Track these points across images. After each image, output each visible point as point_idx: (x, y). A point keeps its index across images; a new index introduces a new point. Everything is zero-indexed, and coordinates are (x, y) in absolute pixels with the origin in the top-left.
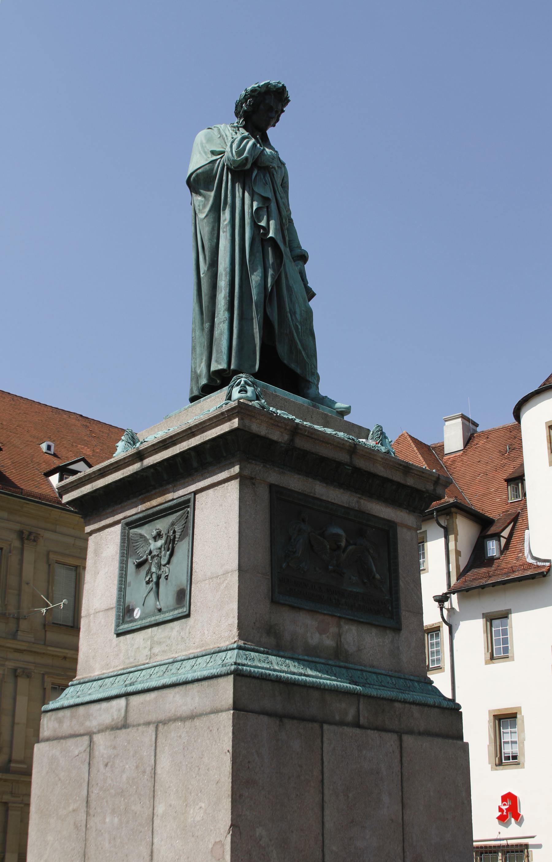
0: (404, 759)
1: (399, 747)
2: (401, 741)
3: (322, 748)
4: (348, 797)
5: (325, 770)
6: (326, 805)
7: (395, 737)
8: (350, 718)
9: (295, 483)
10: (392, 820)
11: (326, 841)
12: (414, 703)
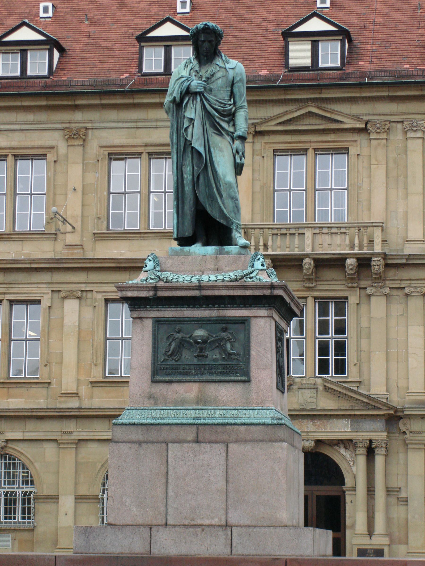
0: (229, 457)
1: (226, 451)
2: (227, 447)
3: (167, 456)
4: (185, 480)
5: (169, 466)
6: (169, 485)
7: (221, 446)
8: (190, 438)
9: (169, 313)
10: (218, 490)
11: (169, 503)
12: (243, 424)
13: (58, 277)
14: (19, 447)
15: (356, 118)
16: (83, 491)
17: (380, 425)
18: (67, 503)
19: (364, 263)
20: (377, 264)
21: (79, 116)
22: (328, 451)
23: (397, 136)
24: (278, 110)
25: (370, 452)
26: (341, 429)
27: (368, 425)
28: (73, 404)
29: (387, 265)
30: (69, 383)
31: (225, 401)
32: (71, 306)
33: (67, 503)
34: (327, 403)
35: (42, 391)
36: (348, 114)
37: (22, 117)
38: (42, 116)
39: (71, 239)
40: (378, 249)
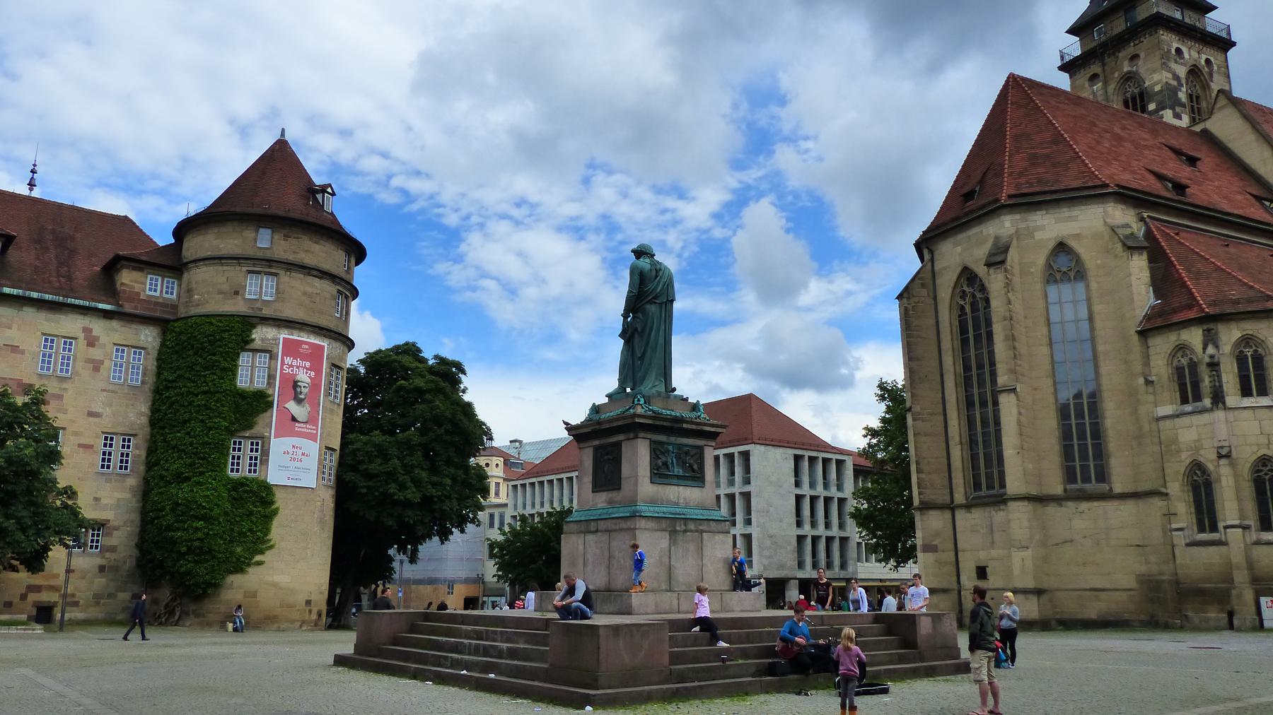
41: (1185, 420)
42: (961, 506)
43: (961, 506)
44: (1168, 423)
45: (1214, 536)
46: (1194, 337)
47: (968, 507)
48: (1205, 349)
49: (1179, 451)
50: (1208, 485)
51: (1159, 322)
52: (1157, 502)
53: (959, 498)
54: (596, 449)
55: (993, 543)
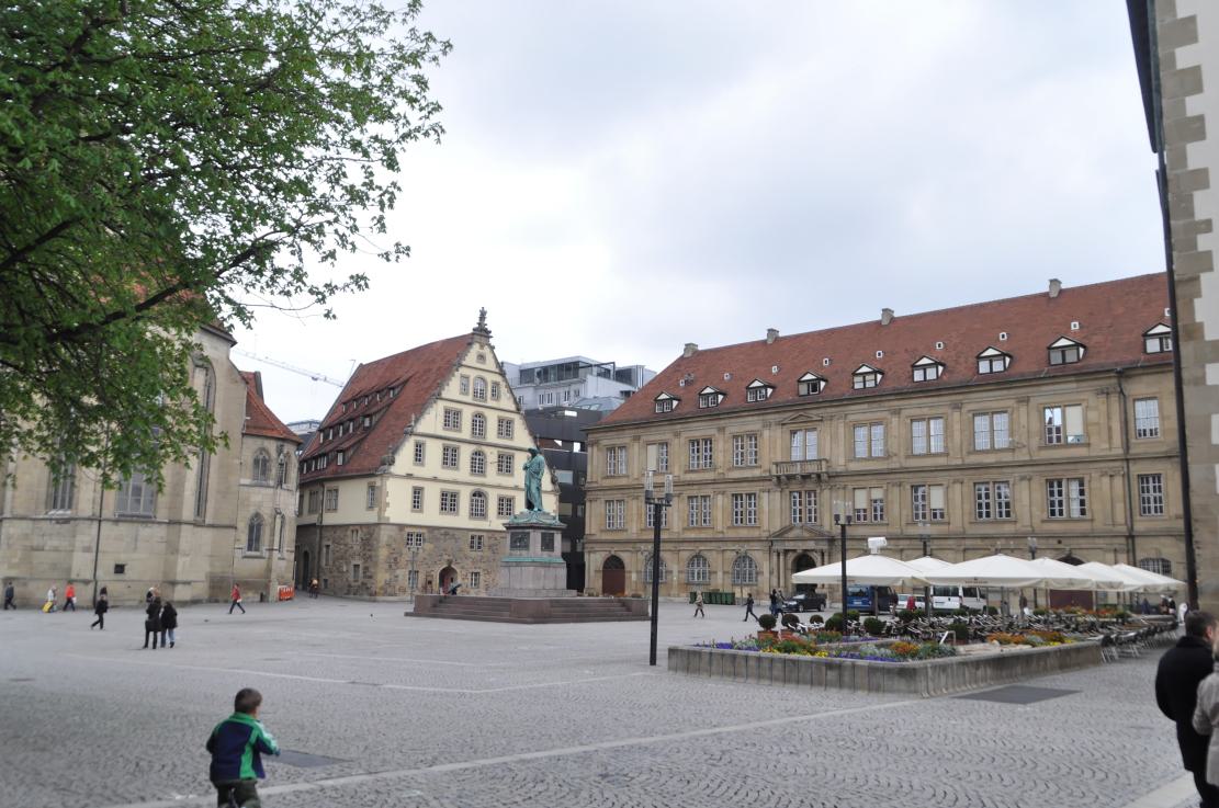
9: (513, 531)
13: (716, 486)
14: (753, 553)
15: (817, 415)
16: (726, 569)
17: (825, 543)
18: (720, 574)
19: (819, 476)
20: (824, 477)
21: (722, 422)
22: (809, 554)
23: (834, 423)
24: (790, 414)
25: (823, 555)
26: (811, 545)
27: (821, 543)
28: (720, 536)
29: (829, 477)
30: (720, 528)
31: (522, 555)
32: (720, 497)
33: (720, 574)
34: (806, 535)
35: (711, 531)
36: (814, 414)
37: (704, 424)
38: (710, 423)
39: (720, 471)
40: (824, 470)
41: (257, 489)
42: (108, 520)
43: (108, 520)
44: (246, 489)
45: (257, 554)
46: (272, 446)
47: (116, 522)
48: (279, 455)
49: (248, 505)
50: (259, 525)
51: (254, 432)
52: (232, 531)
53: (107, 513)
54: (543, 534)
55: (135, 548)
